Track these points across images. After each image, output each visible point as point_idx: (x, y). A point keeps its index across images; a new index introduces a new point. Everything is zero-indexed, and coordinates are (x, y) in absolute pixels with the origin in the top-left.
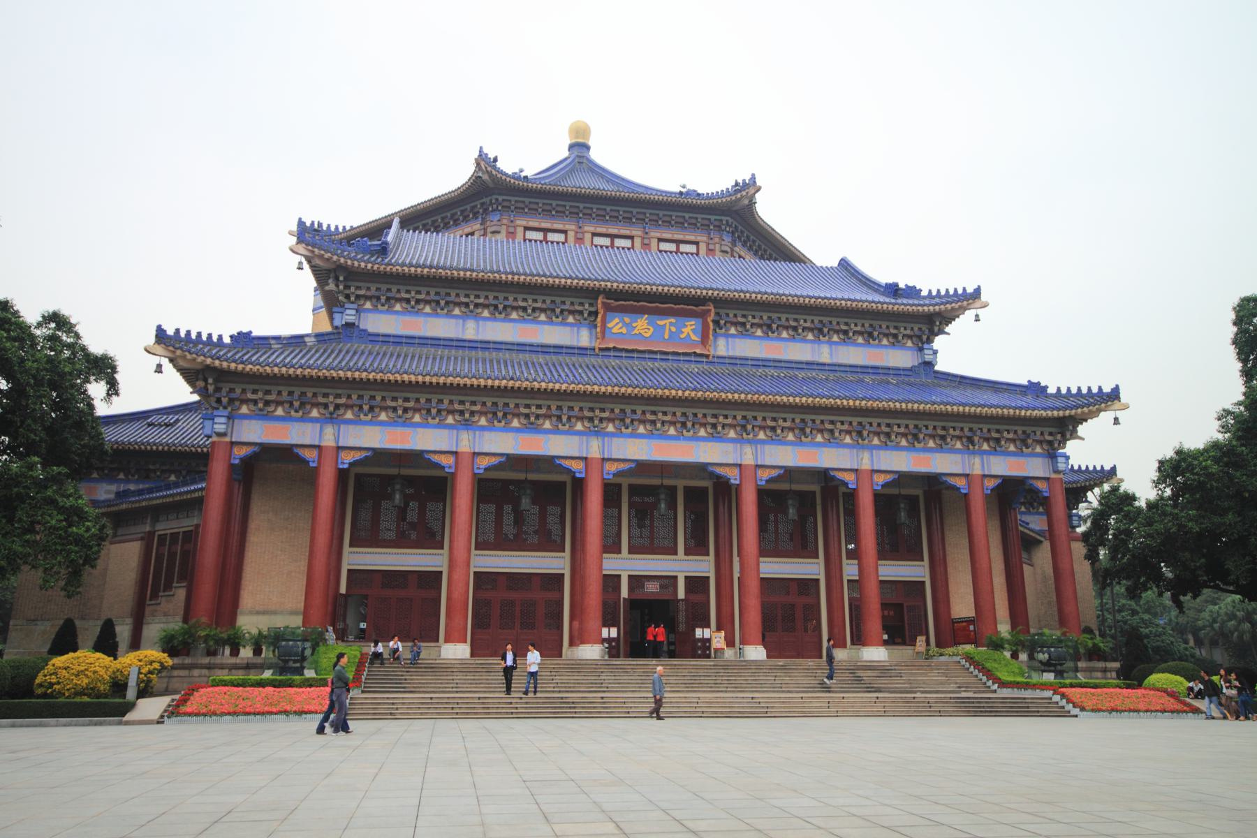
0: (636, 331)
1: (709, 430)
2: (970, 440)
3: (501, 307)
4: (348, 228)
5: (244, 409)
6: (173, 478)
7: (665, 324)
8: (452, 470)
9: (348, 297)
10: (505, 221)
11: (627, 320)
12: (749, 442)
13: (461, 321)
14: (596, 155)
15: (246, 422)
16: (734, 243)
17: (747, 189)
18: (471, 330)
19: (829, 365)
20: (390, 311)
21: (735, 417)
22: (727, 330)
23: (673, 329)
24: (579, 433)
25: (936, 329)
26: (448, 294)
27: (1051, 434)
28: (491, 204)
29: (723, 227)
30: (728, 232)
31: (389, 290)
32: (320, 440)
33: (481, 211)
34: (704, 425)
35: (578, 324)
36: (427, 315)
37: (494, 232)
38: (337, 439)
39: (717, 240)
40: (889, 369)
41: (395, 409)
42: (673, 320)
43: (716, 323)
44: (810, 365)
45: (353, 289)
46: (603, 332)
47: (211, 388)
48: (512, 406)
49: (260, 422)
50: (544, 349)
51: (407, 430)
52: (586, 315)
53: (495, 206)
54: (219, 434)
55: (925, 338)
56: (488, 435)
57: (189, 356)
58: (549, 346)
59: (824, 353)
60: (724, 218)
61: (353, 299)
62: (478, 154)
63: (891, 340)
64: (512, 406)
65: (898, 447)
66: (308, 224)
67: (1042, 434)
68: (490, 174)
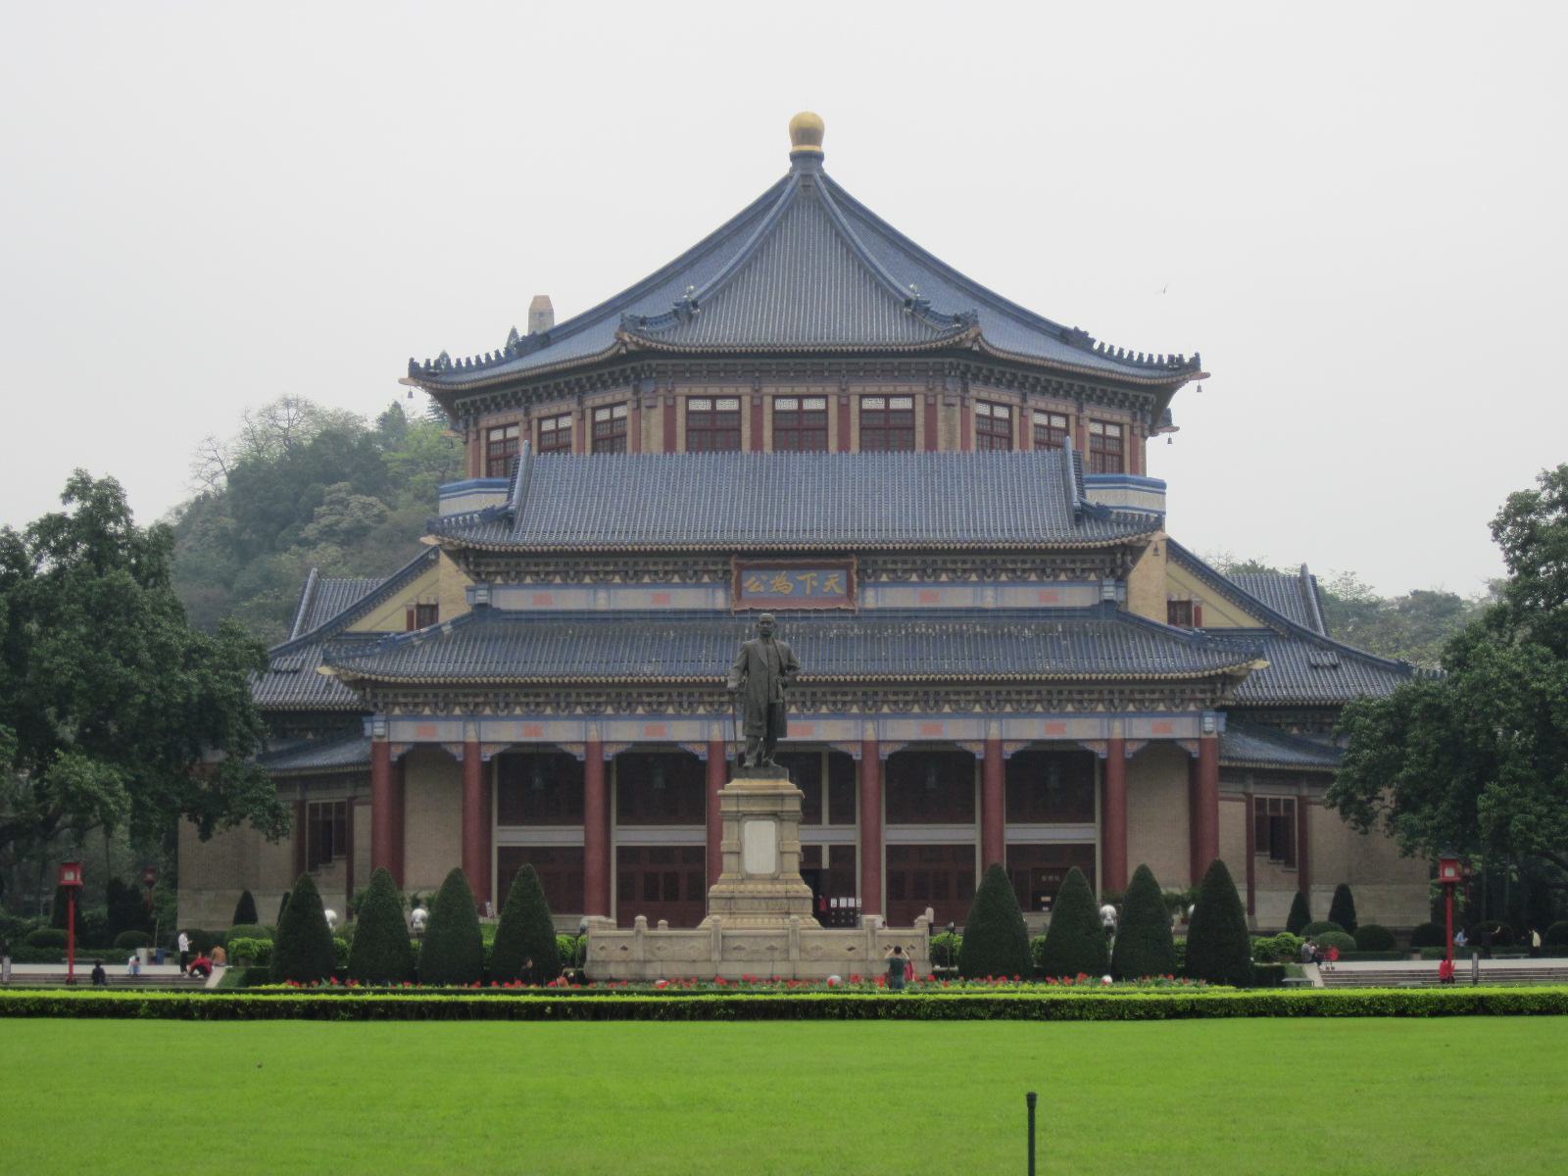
0: (775, 589)
1: (831, 707)
2: (1111, 701)
3: (631, 573)
5: (397, 711)
6: (310, 736)
7: (806, 580)
8: (583, 759)
9: (478, 574)
10: (661, 391)
11: (764, 577)
12: (871, 718)
13: (592, 591)
14: (832, 168)
15: (400, 723)
18: (603, 600)
19: (992, 610)
20: (521, 585)
21: (855, 694)
22: (878, 578)
23: (815, 583)
24: (700, 717)
25: (1119, 562)
26: (577, 564)
27: (1203, 691)
31: (518, 564)
32: (465, 734)
34: (826, 703)
35: (713, 585)
36: (558, 586)
37: (649, 407)
38: (479, 734)
40: (1062, 610)
41: (528, 704)
42: (815, 575)
43: (862, 572)
44: (969, 612)
45: (483, 568)
46: (739, 596)
47: (369, 696)
48: (635, 695)
49: (412, 723)
50: (679, 615)
51: (539, 723)
52: (720, 575)
53: (648, 374)
54: (379, 737)
55: (1108, 571)
56: (613, 724)
57: (350, 674)
58: (682, 612)
59: (989, 598)
61: (483, 576)
63: (1070, 575)
64: (635, 695)
65: (1031, 714)
66: (422, 365)
67: (1193, 691)
68: (637, 343)
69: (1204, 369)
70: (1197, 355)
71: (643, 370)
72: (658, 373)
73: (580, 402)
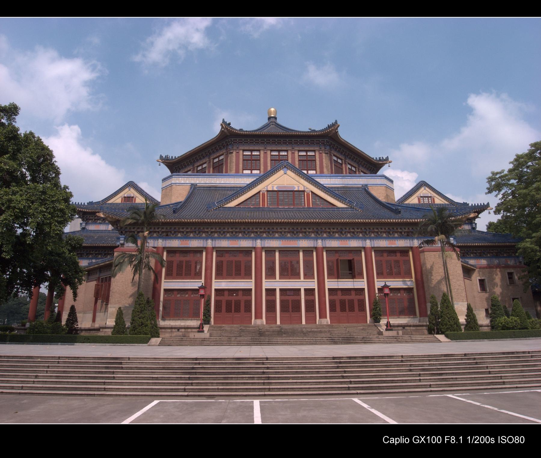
4: (177, 157)
10: (235, 148)
16: (330, 149)
17: (335, 126)
28: (229, 142)
29: (325, 143)
30: (328, 145)
33: (226, 145)
39: (323, 149)
53: (230, 143)
60: (325, 140)
62: (222, 122)
66: (164, 157)
69: (389, 160)
70: (388, 157)
71: (229, 142)
72: (234, 143)
73: (209, 158)
